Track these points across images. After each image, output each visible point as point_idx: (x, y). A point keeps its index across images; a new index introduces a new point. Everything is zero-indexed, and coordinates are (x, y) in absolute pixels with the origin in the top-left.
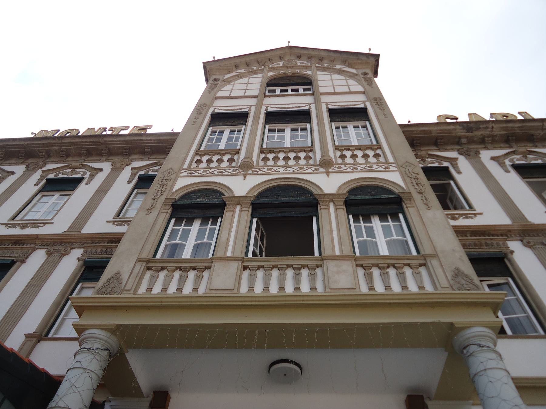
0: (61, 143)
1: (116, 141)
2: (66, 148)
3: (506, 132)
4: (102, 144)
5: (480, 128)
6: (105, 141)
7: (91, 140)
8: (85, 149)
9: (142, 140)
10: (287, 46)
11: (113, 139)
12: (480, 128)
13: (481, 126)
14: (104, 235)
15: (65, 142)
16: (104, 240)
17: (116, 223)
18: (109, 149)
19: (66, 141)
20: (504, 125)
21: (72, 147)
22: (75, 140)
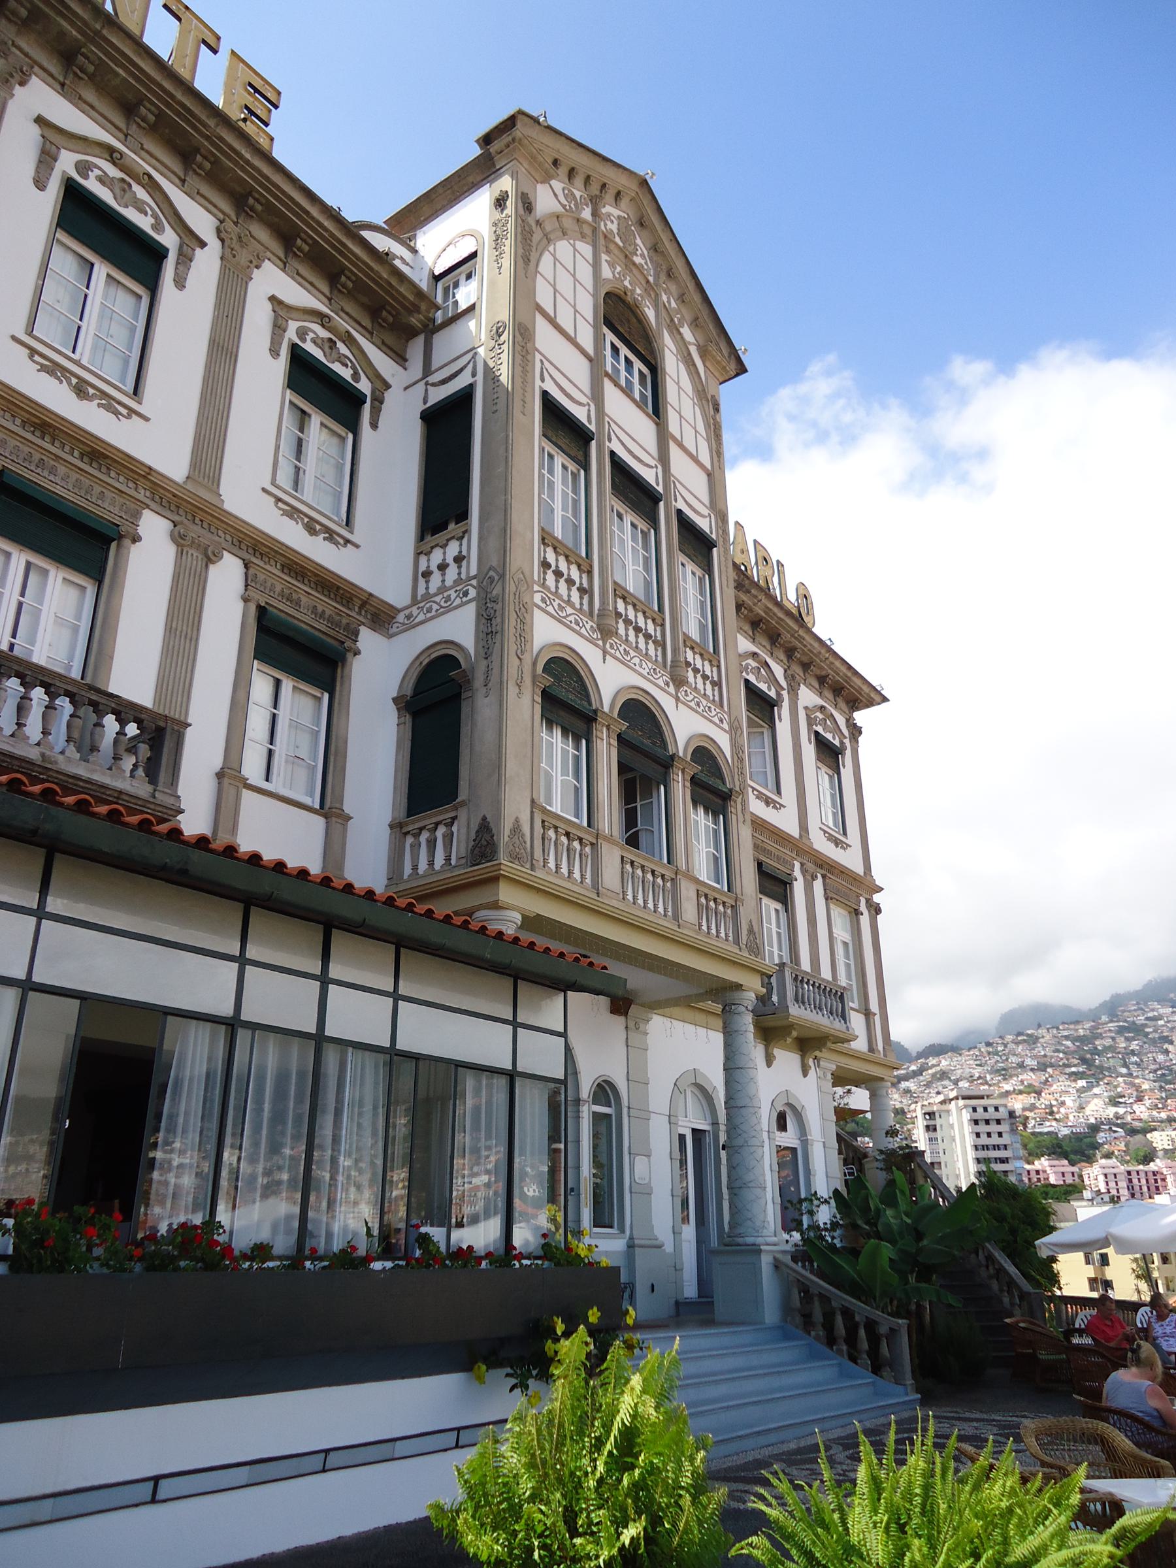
0: (98, 33)
1: (247, 162)
2: (100, 58)
3: (764, 615)
4: (207, 138)
5: (749, 592)
6: (221, 139)
7: (188, 103)
8: (153, 108)
9: (307, 213)
10: (640, 176)
11: (243, 152)
12: (749, 592)
13: (753, 591)
14: (284, 548)
15: (107, 39)
16: (278, 556)
17: (280, 504)
18: (216, 162)
19: (114, 41)
20: (770, 606)
21: (121, 71)
22: (143, 59)
